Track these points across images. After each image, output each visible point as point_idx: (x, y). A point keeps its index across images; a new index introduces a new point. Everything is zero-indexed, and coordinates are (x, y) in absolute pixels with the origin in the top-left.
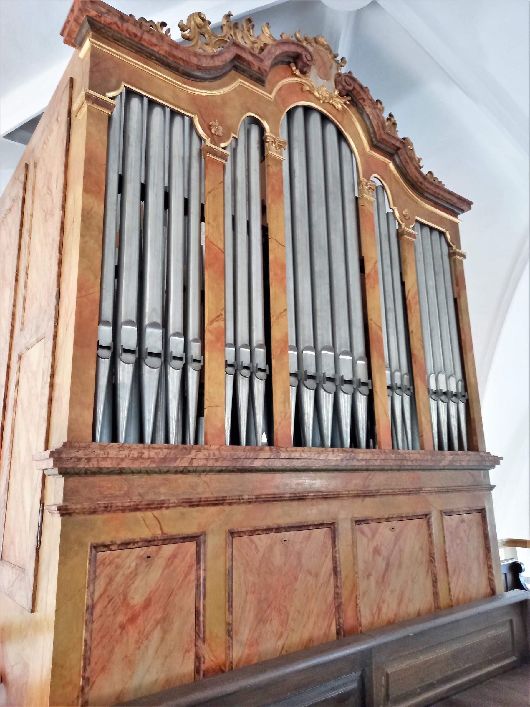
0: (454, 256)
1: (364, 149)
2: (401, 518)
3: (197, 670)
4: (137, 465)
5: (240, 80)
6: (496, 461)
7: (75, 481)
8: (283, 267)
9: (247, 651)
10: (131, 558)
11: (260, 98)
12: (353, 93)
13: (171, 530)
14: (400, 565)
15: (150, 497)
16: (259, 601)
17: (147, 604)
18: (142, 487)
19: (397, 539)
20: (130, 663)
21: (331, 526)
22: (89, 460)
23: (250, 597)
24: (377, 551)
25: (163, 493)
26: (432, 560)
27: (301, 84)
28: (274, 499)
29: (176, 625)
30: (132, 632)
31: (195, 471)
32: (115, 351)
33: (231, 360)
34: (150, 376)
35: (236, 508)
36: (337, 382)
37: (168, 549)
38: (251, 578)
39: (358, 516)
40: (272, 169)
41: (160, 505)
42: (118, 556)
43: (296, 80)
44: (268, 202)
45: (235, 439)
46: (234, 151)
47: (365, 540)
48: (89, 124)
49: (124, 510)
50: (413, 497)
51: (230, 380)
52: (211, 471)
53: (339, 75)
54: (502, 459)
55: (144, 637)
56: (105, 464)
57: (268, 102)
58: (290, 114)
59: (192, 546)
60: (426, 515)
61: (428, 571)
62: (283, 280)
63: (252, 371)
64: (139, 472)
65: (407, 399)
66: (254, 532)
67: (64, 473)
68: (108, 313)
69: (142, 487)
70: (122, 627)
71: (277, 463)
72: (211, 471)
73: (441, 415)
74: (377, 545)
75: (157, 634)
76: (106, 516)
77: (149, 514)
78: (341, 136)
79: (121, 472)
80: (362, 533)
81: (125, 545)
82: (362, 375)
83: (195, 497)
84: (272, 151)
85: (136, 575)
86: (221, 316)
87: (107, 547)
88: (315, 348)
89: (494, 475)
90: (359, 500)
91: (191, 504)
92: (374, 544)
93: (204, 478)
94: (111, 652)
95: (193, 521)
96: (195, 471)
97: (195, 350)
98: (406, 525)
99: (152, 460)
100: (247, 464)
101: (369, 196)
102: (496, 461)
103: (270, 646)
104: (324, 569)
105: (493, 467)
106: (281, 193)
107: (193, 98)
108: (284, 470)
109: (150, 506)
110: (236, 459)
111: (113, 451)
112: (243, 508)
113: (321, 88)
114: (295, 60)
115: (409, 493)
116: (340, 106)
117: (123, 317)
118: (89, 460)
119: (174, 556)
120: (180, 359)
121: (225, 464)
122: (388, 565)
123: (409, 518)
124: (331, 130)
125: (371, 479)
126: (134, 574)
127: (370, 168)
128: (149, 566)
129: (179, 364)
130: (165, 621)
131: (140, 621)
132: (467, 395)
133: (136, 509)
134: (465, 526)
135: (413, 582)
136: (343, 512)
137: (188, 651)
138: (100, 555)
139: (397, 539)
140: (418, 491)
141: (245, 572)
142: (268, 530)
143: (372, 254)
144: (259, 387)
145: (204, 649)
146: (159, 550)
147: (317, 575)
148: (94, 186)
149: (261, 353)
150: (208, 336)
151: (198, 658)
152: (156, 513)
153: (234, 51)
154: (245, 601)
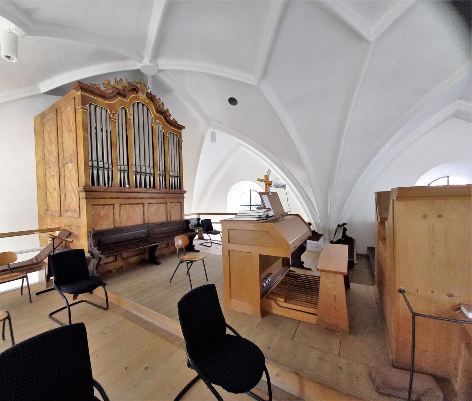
2: (160, 203)
4: (100, 190)
5: (119, 98)
6: (186, 192)
7: (88, 193)
8: (132, 146)
10: (100, 207)
11: (125, 101)
12: (151, 97)
13: (107, 203)
15: (103, 196)
17: (104, 215)
21: (143, 204)
26: (167, 212)
27: (136, 97)
28: (130, 198)
32: (93, 167)
33: (119, 169)
34: (101, 172)
35: (121, 200)
36: (146, 174)
37: (107, 206)
40: (128, 121)
43: (135, 95)
45: (121, 186)
46: (118, 116)
48: (82, 115)
51: (119, 173)
52: (116, 192)
53: (147, 92)
56: (93, 190)
57: (127, 103)
58: (133, 105)
59: (112, 206)
62: (132, 150)
63: (124, 171)
65: (164, 177)
66: (125, 204)
67: (85, 191)
68: (90, 159)
72: (116, 192)
73: (172, 181)
77: (103, 200)
78: (148, 109)
79: (97, 191)
81: (98, 205)
82: (152, 172)
84: (128, 116)
87: (95, 205)
91: (111, 198)
93: (114, 193)
97: (110, 166)
100: (123, 191)
101: (155, 127)
102: (186, 192)
103: (129, 224)
106: (131, 127)
107: (107, 104)
108: (132, 192)
111: (99, 187)
112: (123, 200)
113: (142, 96)
114: (135, 90)
117: (94, 159)
121: (118, 191)
122: (156, 212)
126: (101, 210)
127: (156, 118)
129: (107, 170)
132: (180, 177)
133: (100, 198)
136: (146, 202)
140: (164, 198)
142: (128, 204)
143: (156, 142)
144: (126, 175)
145: (116, 224)
148: (85, 129)
149: (126, 167)
151: (114, 226)
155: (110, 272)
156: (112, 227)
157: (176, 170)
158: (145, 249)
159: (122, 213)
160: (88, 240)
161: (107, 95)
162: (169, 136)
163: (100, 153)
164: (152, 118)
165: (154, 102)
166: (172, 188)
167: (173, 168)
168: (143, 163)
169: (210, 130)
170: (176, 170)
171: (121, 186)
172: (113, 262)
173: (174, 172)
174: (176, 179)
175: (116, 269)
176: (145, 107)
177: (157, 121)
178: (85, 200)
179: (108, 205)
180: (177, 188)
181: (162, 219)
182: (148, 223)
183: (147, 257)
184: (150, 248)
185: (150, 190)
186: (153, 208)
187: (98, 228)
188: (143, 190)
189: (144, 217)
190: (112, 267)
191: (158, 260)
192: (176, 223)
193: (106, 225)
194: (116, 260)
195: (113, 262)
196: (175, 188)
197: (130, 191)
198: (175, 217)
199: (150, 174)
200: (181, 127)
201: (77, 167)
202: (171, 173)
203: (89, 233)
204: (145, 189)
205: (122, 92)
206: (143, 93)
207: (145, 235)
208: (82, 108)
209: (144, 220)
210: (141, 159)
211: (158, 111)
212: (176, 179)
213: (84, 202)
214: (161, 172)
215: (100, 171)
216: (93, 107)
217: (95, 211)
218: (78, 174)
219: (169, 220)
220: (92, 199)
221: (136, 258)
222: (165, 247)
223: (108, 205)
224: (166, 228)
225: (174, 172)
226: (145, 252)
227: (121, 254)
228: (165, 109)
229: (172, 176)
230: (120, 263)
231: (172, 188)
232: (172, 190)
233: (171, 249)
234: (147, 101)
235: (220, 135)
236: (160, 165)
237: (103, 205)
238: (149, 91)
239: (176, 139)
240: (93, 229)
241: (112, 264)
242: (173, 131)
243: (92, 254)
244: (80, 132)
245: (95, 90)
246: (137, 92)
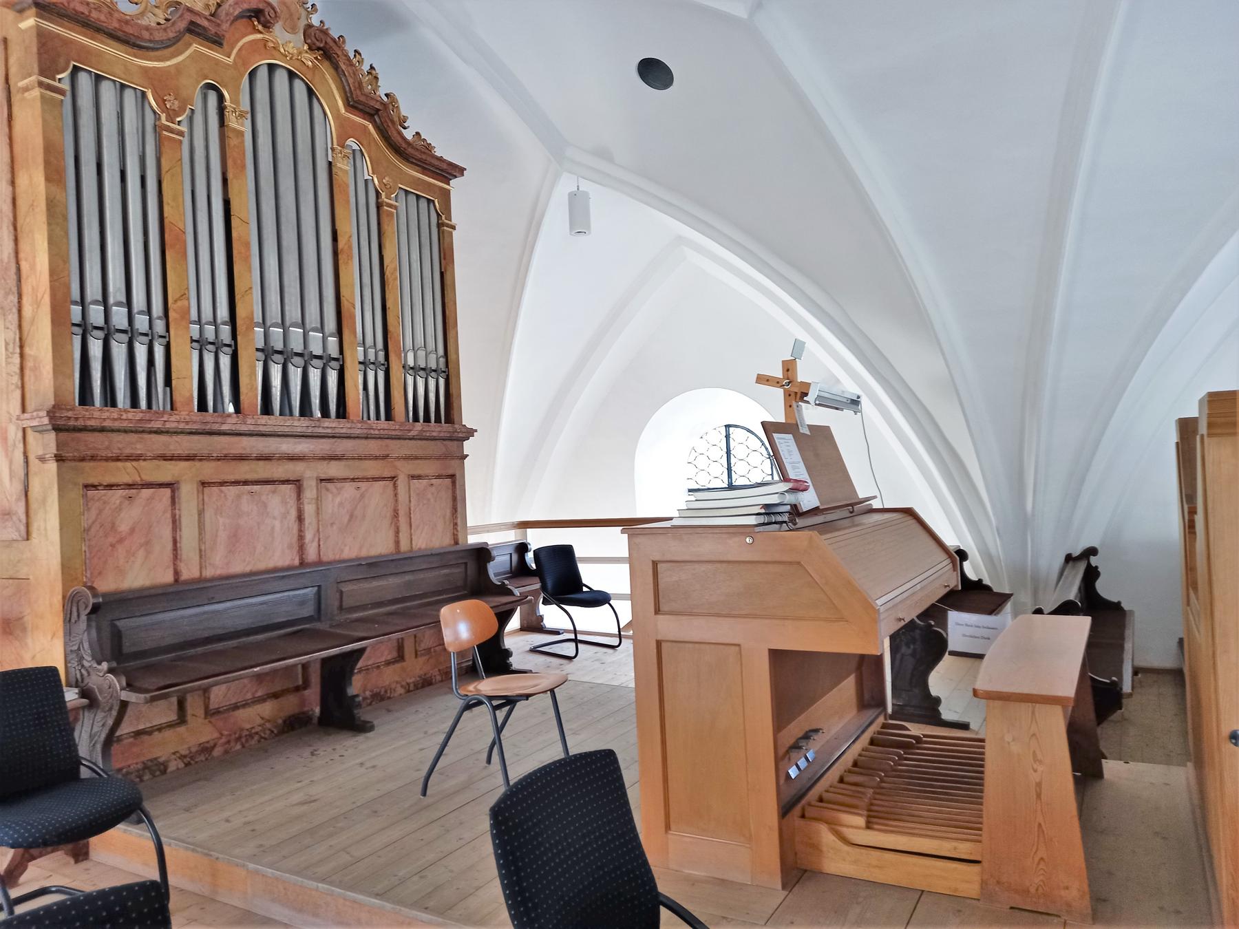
0: (443, 228)
1: (338, 110)
2: (367, 479)
3: (176, 581)
4: (117, 425)
5: (195, 46)
6: (470, 433)
7: (64, 435)
8: (247, 245)
11: (217, 62)
12: (325, 47)
13: (148, 478)
15: (128, 451)
17: (132, 530)
18: (120, 443)
19: (362, 496)
20: (121, 572)
21: (297, 483)
22: (77, 419)
25: (139, 449)
26: (396, 514)
27: (265, 41)
28: (241, 458)
30: (121, 550)
31: (167, 432)
32: (85, 328)
35: (206, 464)
36: (307, 358)
37: (146, 493)
40: (232, 141)
41: (138, 458)
43: (259, 36)
44: (230, 176)
45: (202, 406)
46: (191, 119)
48: (43, 111)
49: (107, 459)
50: (380, 462)
51: (196, 354)
52: (182, 432)
53: (310, 26)
56: (89, 423)
58: (252, 75)
59: (168, 491)
62: (247, 259)
63: (218, 346)
64: (119, 431)
65: (381, 375)
66: (222, 484)
67: (57, 429)
68: (76, 294)
69: (120, 443)
70: (113, 546)
71: (244, 428)
72: (182, 432)
73: (416, 388)
75: (141, 553)
76: (92, 464)
77: (128, 464)
79: (102, 430)
81: (110, 487)
82: (333, 351)
83: (168, 453)
84: (232, 122)
86: (184, 296)
87: (95, 487)
88: (283, 324)
89: (468, 446)
91: (165, 458)
94: (105, 562)
95: (167, 472)
96: (167, 432)
100: (216, 427)
101: (343, 166)
102: (470, 433)
103: (238, 567)
106: (243, 167)
107: (146, 70)
108: (251, 434)
109: (129, 458)
112: (213, 464)
113: (287, 41)
115: (376, 458)
118: (77, 419)
119: (152, 498)
120: (146, 335)
121: (196, 427)
122: (351, 516)
124: (299, 87)
126: (119, 509)
129: (146, 339)
130: (147, 544)
132: (448, 372)
133: (117, 459)
134: (433, 489)
136: (309, 472)
139: (362, 496)
140: (385, 457)
142: (236, 483)
143: (347, 228)
144: (225, 361)
148: (53, 175)
149: (226, 330)
150: (172, 314)
151: (177, 573)
152: (135, 463)
153: (188, 17)
155: (158, 768)
156: (168, 578)
157: (431, 345)
158: (305, 666)
159: (208, 515)
160: (68, 633)
161: (146, 35)
162: (401, 206)
163: (114, 273)
164: (328, 131)
165: (336, 67)
166: (416, 419)
167: (416, 336)
168: (293, 313)
169: (566, 186)
170: (431, 345)
171: (202, 406)
172: (170, 725)
173: (421, 354)
174: (432, 383)
175: (182, 757)
176: (297, 83)
177: (351, 142)
178: (52, 466)
180: (438, 420)
181: (379, 544)
182: (320, 563)
183: (312, 701)
184: (324, 661)
185: (326, 423)
186: (338, 500)
187: (108, 584)
188: (300, 424)
189: (301, 537)
190: (167, 746)
191: (364, 714)
192: (439, 558)
193: (139, 572)
194: (182, 719)
195: (170, 725)
196: (427, 419)
198: (427, 536)
199: (325, 360)
200: (449, 171)
201: (14, 326)
202: (410, 356)
203: (70, 602)
204: (305, 422)
205: (205, 23)
206: (293, 30)
207: (309, 610)
208: (41, 84)
209: (302, 548)
210: (286, 303)
211: (353, 105)
212: (432, 383)
213: (47, 476)
214: (371, 352)
215: (114, 344)
216: (84, 81)
217: (94, 513)
218: (22, 355)
219: (404, 546)
220: (83, 460)
221: (267, 709)
222: (388, 663)
224: (393, 581)
225: (421, 354)
226: (306, 685)
227: (206, 690)
228: (382, 92)
229: (415, 369)
230: (199, 732)
231: (416, 419)
232: (419, 426)
233: (415, 667)
234: (309, 59)
235: (601, 200)
236: (365, 323)
237: (130, 486)
238: (315, 20)
239: (428, 218)
240: (91, 588)
241: (168, 734)
242: (417, 183)
243: (85, 693)
244: (34, 181)
245: (94, 14)
246: (267, 26)
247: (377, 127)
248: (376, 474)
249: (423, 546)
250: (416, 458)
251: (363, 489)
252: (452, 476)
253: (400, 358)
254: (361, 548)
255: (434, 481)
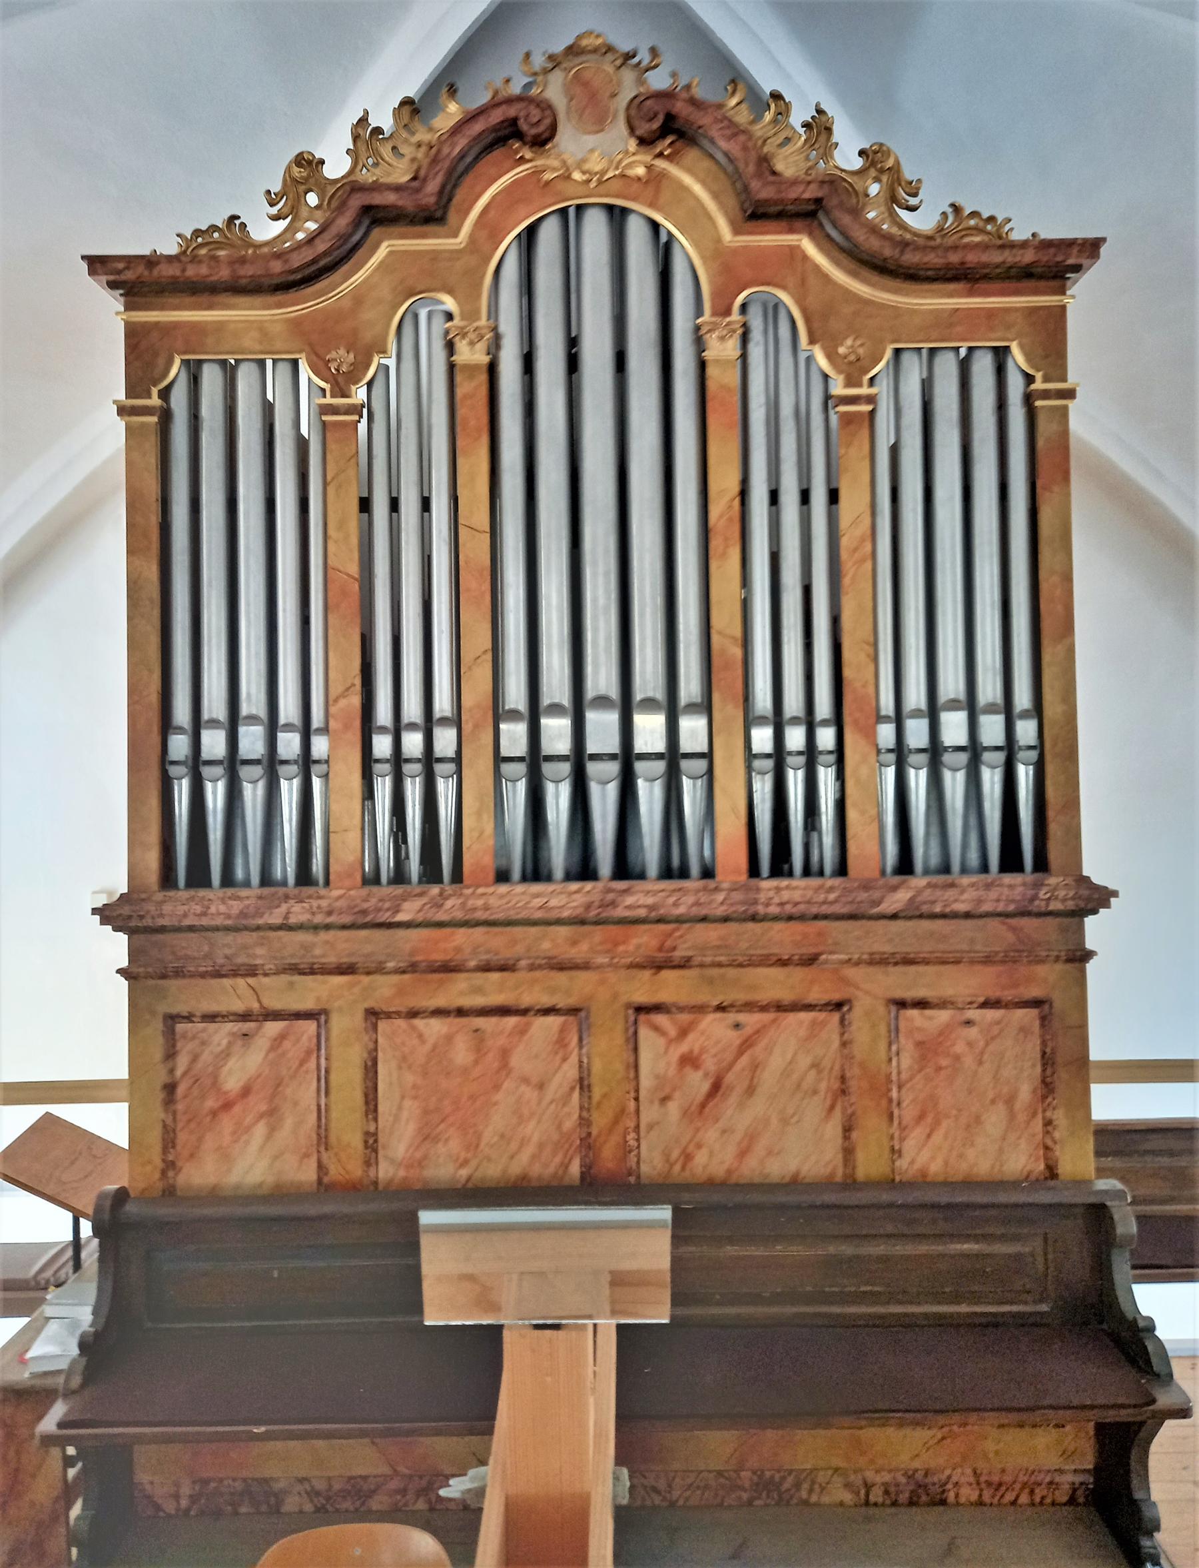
1: (718, 240)
3: (320, 1181)
7: (141, 938)
9: (402, 1173)
10: (222, 1033)
13: (275, 1003)
14: (751, 1091)
16: (426, 1112)
17: (246, 1091)
18: (227, 947)
19: (746, 1045)
20: (226, 1157)
22: (141, 917)
23: (408, 1103)
24: (689, 1061)
25: (260, 955)
29: (289, 1122)
30: (227, 1123)
37: (273, 1028)
38: (410, 1078)
39: (641, 998)
41: (252, 971)
42: (204, 1030)
47: (661, 1041)
49: (203, 975)
54: (1115, 894)
55: (242, 1131)
57: (456, 254)
59: (310, 1027)
60: (839, 1005)
61: (832, 1108)
66: (413, 1014)
70: (214, 1114)
74: (691, 1052)
75: (260, 1130)
77: (240, 982)
80: (656, 1028)
81: (211, 1018)
85: (228, 1055)
87: (189, 1018)
90: (646, 974)
91: (295, 969)
92: (684, 1048)
93: (323, 936)
94: (200, 1139)
95: (309, 992)
98: (774, 1021)
99: (229, 917)
100: (384, 917)
102: (1098, 898)
104: (557, 1079)
105: (1094, 912)
109: (235, 973)
110: (364, 912)
113: (592, 151)
115: (783, 963)
116: (640, 171)
118: (141, 917)
119: (282, 1037)
122: (716, 1087)
123: (781, 1008)
125: (681, 936)
126: (226, 1054)
128: (246, 1046)
130: (272, 1114)
131: (237, 1109)
133: (218, 975)
134: (973, 1032)
135: (785, 1121)
137: (307, 1155)
138: (180, 1027)
139: (746, 1045)
141: (400, 1068)
142: (439, 1012)
146: (259, 1028)
147: (541, 1086)
151: (320, 1166)
152: (251, 980)
154: (400, 1108)
168: (602, 676)
175: (313, 1493)
179: (276, 1016)
197: (441, 916)
209: (587, 1144)
223: (276, 1016)
237: (245, 1017)
242: (947, 323)
247: (826, 243)
248: (787, 996)
249: (935, 1168)
250: (908, 961)
251: (748, 1031)
252: (1037, 1003)
253: (871, 736)
254: (743, 1154)
255: (972, 1014)
